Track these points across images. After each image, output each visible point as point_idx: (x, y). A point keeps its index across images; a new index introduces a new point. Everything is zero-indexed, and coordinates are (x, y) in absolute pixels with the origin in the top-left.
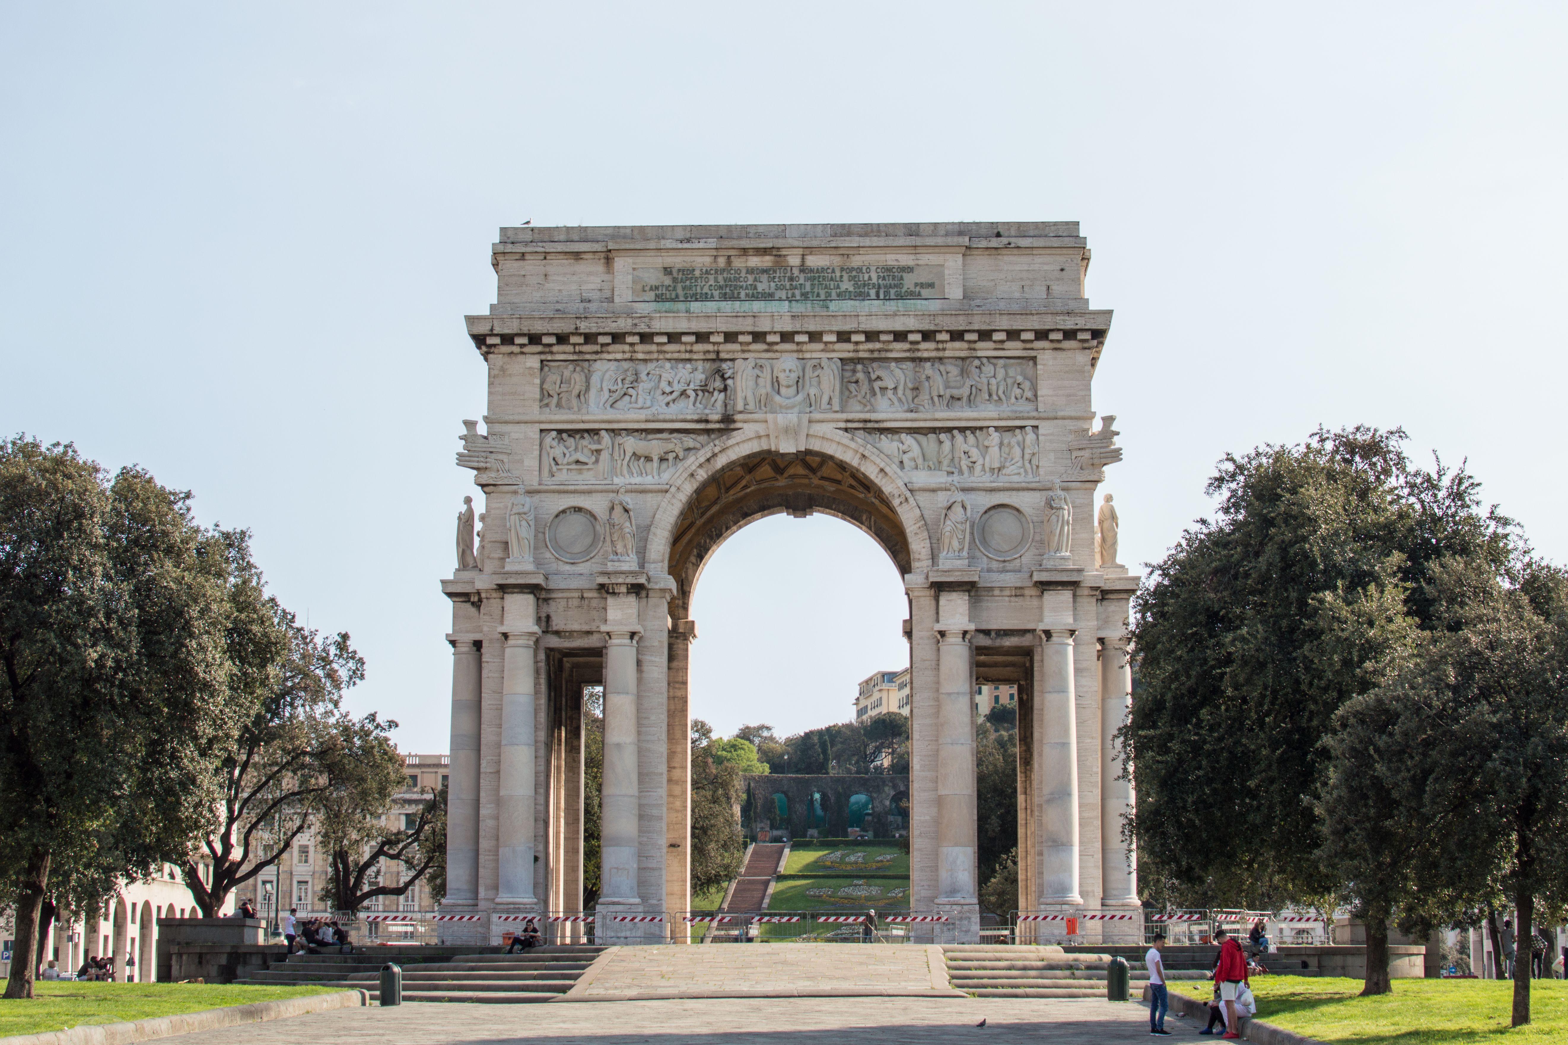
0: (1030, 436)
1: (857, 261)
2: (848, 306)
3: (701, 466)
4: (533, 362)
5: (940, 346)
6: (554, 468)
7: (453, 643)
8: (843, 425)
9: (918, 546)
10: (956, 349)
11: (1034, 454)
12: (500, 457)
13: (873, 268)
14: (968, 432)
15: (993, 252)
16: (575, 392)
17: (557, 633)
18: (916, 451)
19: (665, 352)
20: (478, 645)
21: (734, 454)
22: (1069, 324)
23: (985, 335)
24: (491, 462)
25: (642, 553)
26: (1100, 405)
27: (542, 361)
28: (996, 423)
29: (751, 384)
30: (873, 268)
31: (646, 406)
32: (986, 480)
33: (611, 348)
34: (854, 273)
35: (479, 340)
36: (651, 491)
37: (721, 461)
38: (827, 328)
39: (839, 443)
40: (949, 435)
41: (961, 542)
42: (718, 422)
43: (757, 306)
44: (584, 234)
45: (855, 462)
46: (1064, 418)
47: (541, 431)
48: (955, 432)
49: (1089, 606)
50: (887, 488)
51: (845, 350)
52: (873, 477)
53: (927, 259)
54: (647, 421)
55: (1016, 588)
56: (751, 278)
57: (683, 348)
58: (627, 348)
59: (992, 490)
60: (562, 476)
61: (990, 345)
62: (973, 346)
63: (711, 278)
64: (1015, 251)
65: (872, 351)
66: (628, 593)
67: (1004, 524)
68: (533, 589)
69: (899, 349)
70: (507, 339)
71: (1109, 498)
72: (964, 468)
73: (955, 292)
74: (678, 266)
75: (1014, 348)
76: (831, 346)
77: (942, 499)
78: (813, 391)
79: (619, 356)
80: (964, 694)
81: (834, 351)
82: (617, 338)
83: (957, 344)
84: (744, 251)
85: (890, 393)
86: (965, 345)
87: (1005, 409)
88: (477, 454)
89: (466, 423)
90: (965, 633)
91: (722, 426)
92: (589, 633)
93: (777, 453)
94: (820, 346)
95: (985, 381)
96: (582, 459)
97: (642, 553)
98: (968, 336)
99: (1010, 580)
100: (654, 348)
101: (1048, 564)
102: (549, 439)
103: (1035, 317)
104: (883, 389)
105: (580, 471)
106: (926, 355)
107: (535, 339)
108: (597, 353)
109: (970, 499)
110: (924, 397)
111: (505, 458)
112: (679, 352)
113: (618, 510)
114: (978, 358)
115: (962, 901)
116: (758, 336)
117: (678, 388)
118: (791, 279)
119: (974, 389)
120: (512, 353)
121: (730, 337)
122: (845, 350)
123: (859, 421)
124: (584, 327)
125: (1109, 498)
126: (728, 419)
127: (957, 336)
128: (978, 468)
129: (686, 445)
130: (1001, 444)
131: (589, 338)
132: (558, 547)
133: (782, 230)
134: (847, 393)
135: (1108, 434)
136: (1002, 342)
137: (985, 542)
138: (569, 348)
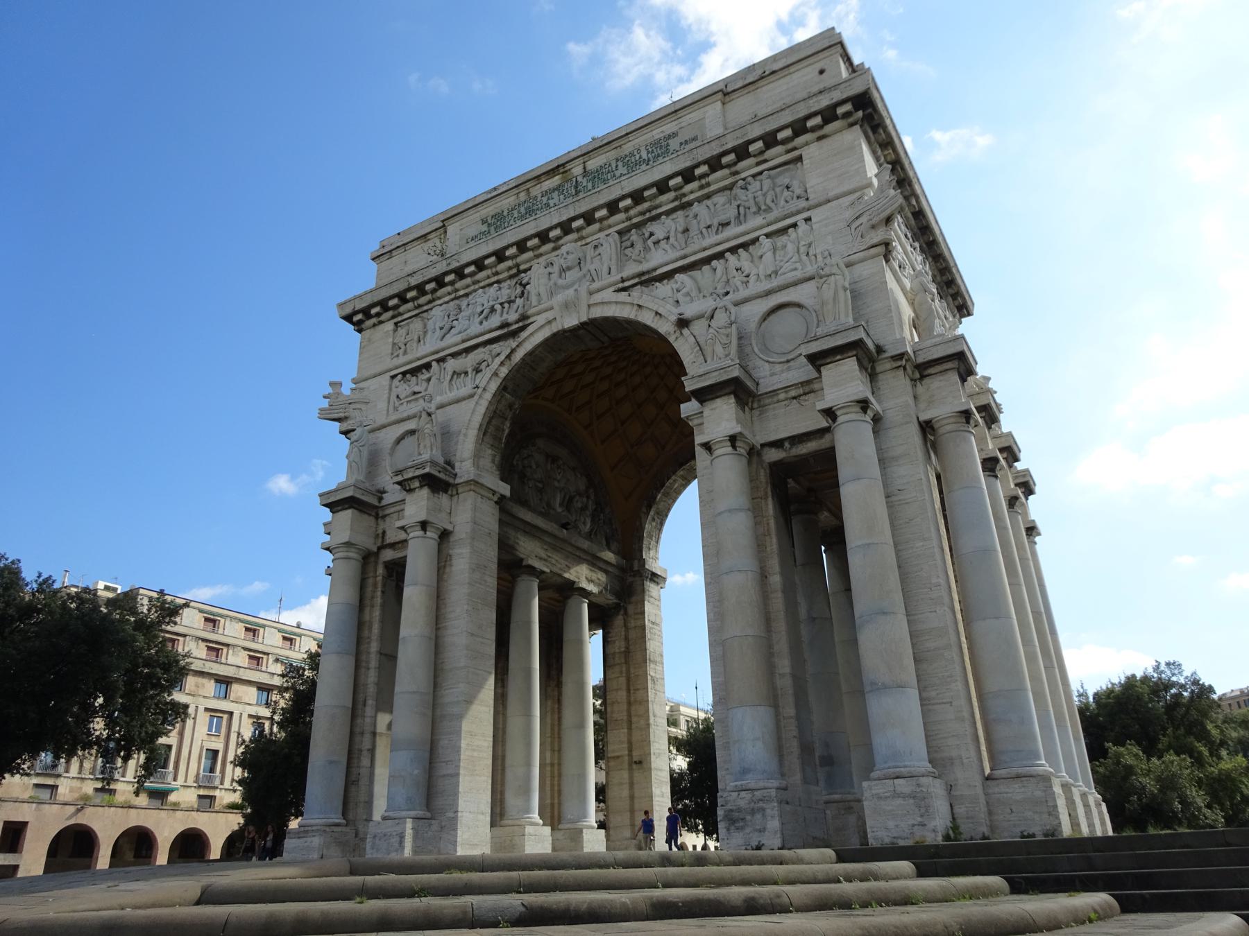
1: (628, 148)
3: (502, 364)
4: (389, 326)
5: (703, 181)
6: (397, 404)
8: (621, 285)
10: (719, 178)
11: (810, 245)
12: (358, 406)
13: (643, 149)
14: (740, 251)
15: (752, 88)
16: (416, 338)
17: (392, 546)
19: (479, 281)
21: (528, 346)
22: (824, 101)
23: (742, 152)
24: (351, 411)
27: (396, 324)
28: (766, 230)
29: (544, 280)
30: (643, 149)
33: (439, 293)
35: (348, 318)
36: (464, 399)
38: (596, 204)
39: (616, 303)
40: (722, 261)
41: (726, 346)
42: (517, 322)
45: (632, 317)
46: (838, 198)
47: (393, 377)
48: (728, 255)
52: (649, 323)
54: (463, 341)
55: (802, 383)
56: (545, 199)
57: (488, 272)
58: (449, 288)
59: (768, 293)
61: (751, 161)
62: (734, 169)
63: (515, 213)
64: (772, 78)
65: (643, 213)
66: (421, 487)
70: (366, 311)
72: (739, 283)
74: (492, 213)
75: (777, 154)
76: (606, 223)
78: (592, 268)
79: (446, 299)
80: (740, 510)
81: (610, 227)
83: (719, 174)
84: (537, 178)
85: (663, 243)
86: (726, 171)
89: (331, 384)
90: (733, 439)
91: (521, 324)
93: (564, 331)
94: (596, 226)
95: (750, 196)
96: (417, 389)
100: (468, 280)
103: (787, 111)
104: (657, 243)
105: (416, 400)
106: (692, 197)
107: (383, 304)
108: (430, 302)
110: (694, 232)
111: (363, 407)
112: (488, 277)
114: (744, 179)
115: (752, 785)
116: (543, 236)
119: (741, 209)
120: (374, 325)
121: (521, 246)
123: (633, 278)
124: (414, 281)
126: (524, 317)
128: (752, 279)
129: (494, 353)
130: (775, 250)
131: (420, 288)
134: (624, 258)
136: (762, 153)
138: (410, 305)
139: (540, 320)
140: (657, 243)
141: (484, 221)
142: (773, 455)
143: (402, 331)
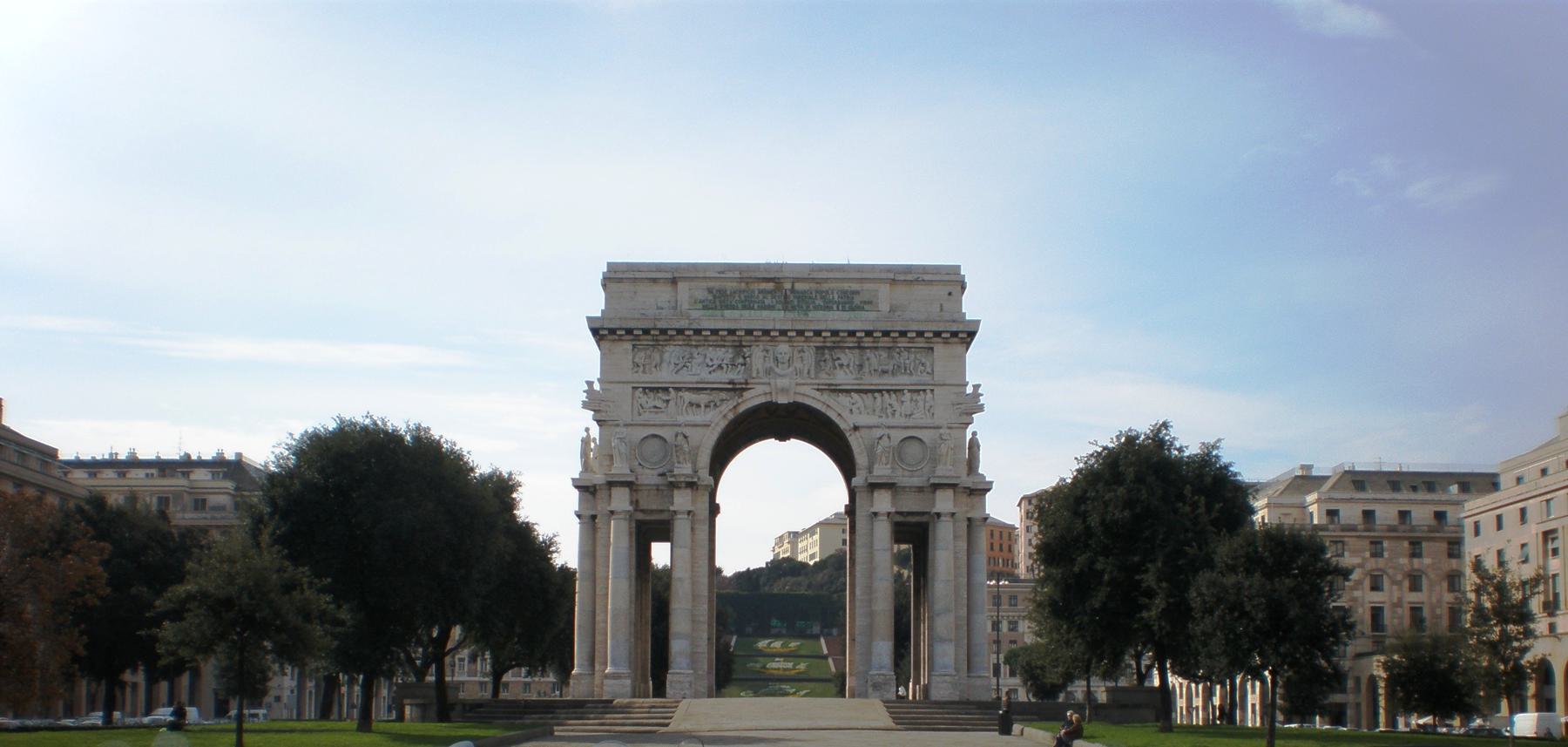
0: (929, 395)
1: (825, 286)
2: (820, 314)
4: (628, 346)
7: (579, 516)
9: (861, 460)
17: (643, 511)
18: (860, 403)
20: (594, 517)
23: (903, 334)
25: (694, 463)
26: (971, 378)
31: (698, 373)
32: (902, 421)
34: (824, 294)
37: (741, 409)
43: (765, 313)
44: (659, 267)
45: (823, 409)
49: (964, 499)
50: (842, 426)
51: (818, 342)
53: (867, 286)
60: (646, 416)
67: (913, 450)
68: (629, 484)
69: (851, 342)
70: (612, 331)
71: (974, 434)
73: (884, 307)
75: (921, 343)
77: (878, 433)
82: (680, 331)
87: (914, 379)
88: (594, 402)
92: (662, 511)
97: (694, 463)
98: (892, 338)
99: (916, 481)
101: (939, 473)
102: (638, 393)
104: (841, 366)
107: (629, 331)
109: (893, 433)
110: (866, 370)
113: (680, 438)
116: (766, 332)
117: (716, 362)
118: (786, 296)
121: (749, 332)
122: (818, 342)
124: (659, 325)
125: (974, 434)
127: (886, 334)
131: (663, 331)
132: (644, 459)
133: (781, 267)
135: (976, 395)
137: (902, 460)
139: (760, 389)
140: (841, 366)
141: (710, 291)
142: (899, 519)
143: (642, 354)
